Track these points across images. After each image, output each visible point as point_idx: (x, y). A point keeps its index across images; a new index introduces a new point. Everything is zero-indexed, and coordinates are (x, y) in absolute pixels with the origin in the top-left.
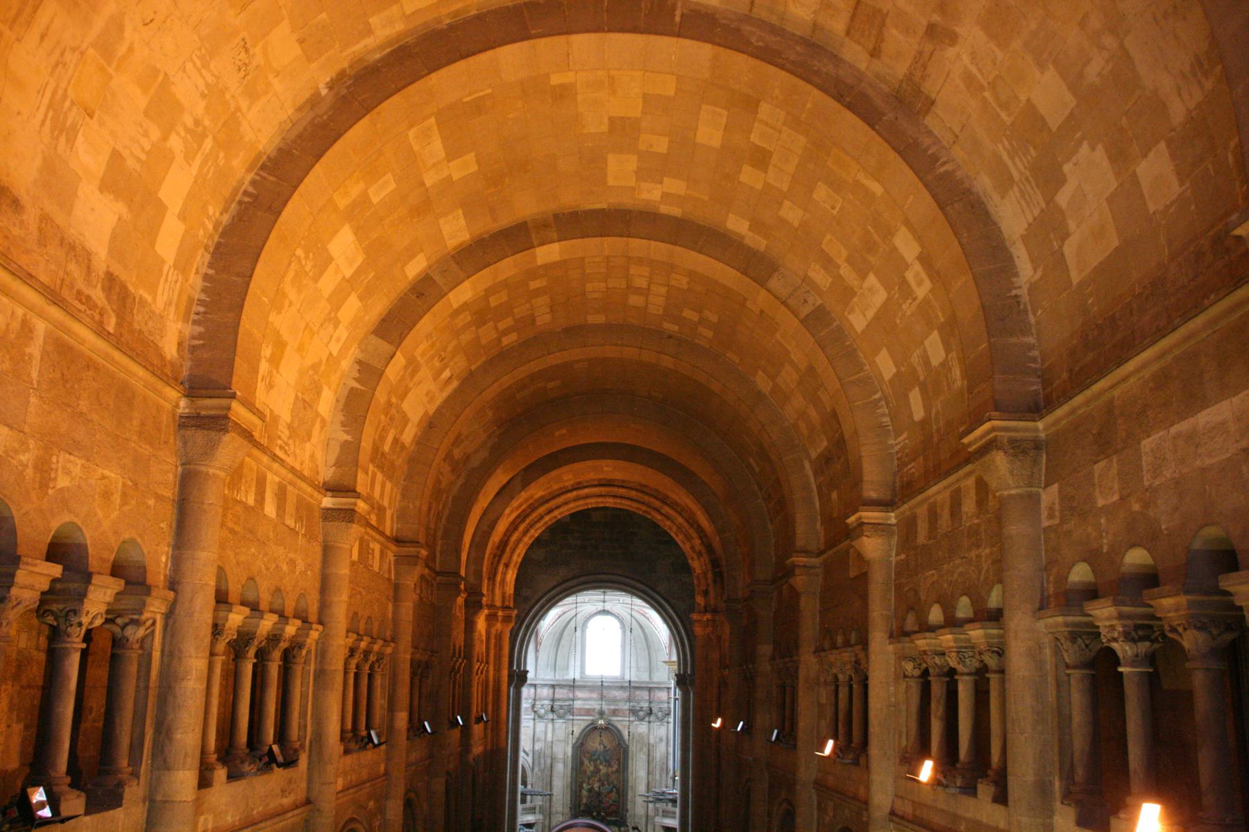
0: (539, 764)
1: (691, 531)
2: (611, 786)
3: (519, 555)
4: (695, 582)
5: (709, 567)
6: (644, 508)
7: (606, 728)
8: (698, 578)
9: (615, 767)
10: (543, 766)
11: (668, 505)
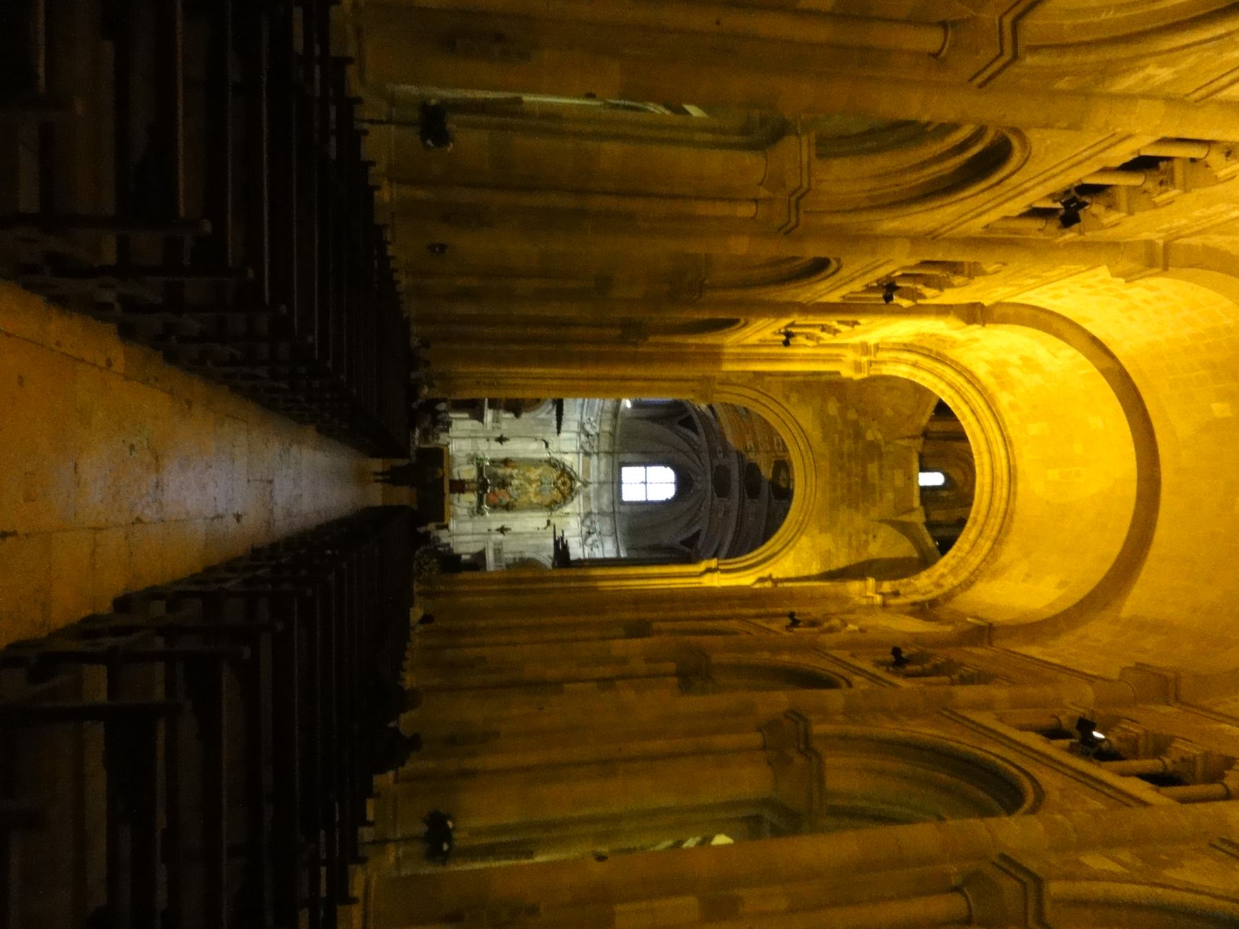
1: (964, 575)
2: (516, 497)
4: (905, 581)
5: (929, 596)
6: (981, 519)
7: (571, 489)
8: (908, 584)
9: (534, 500)
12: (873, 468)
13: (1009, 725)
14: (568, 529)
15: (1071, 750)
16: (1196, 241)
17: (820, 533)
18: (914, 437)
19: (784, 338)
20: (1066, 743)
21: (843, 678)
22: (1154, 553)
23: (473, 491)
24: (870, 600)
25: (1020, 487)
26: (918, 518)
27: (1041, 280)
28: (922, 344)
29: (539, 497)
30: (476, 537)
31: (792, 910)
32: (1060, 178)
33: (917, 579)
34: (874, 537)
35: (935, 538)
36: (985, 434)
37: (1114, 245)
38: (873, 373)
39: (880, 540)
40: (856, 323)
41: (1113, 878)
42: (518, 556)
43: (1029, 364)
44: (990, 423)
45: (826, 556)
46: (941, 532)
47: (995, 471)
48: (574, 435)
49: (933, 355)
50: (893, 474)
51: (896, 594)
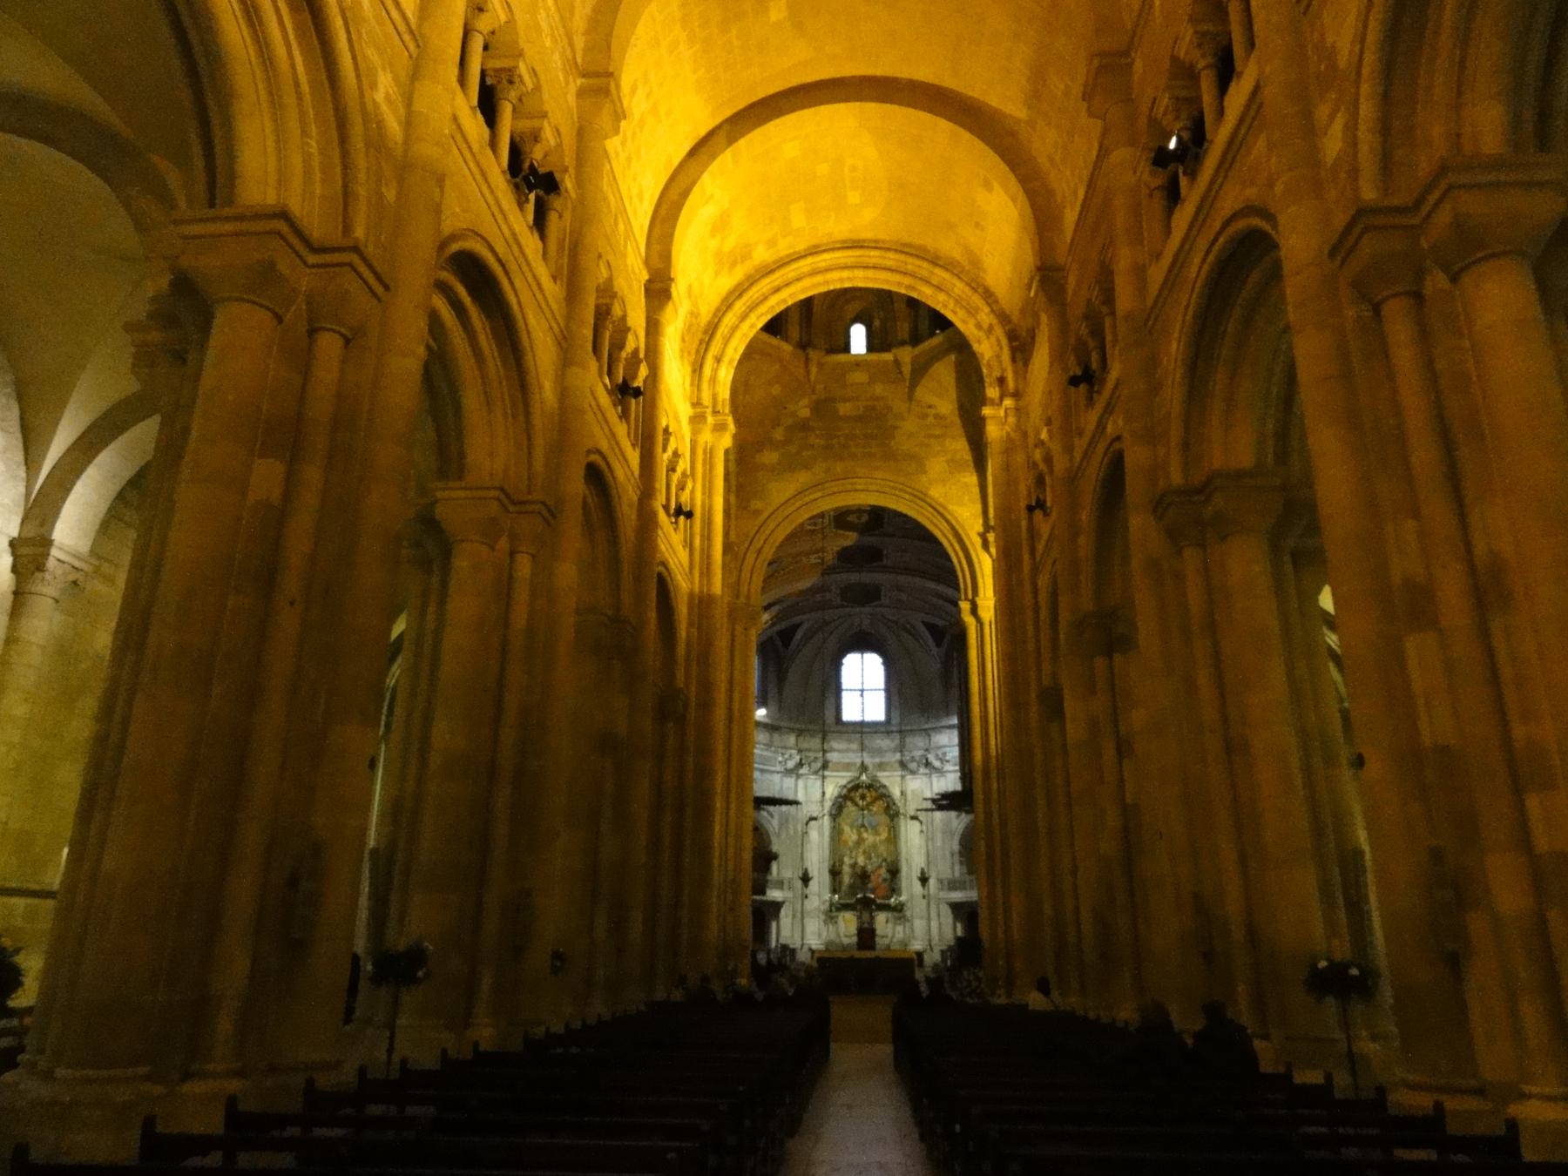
0: (787, 828)
1: (977, 300)
2: (880, 860)
3: (736, 350)
4: (985, 371)
5: (1004, 341)
6: (907, 280)
7: (869, 787)
8: (989, 366)
9: (884, 835)
10: (792, 832)
11: (941, 266)
12: (845, 409)
13: (1165, 242)
14: (922, 792)
15: (1193, 175)
16: (580, 42)
17: (925, 472)
18: (807, 361)
19: (682, 518)
20: (1183, 181)
21: (1108, 449)
22: (949, 82)
23: (872, 918)
24: (1008, 411)
25: (867, 235)
26: (906, 354)
27: (619, 216)
28: (693, 351)
29: (881, 830)
30: (933, 914)
31: (1416, 514)
32: (500, 195)
33: (982, 355)
34: (930, 407)
35: (932, 334)
36: (805, 276)
37: (581, 133)
38: (727, 410)
39: (932, 400)
40: (666, 431)
41: (1351, 128)
42: (957, 858)
43: (720, 226)
44: (790, 272)
45: (955, 466)
46: (924, 325)
47: (850, 264)
48: (801, 783)
49: (707, 339)
50: (852, 385)
51: (1001, 381)
